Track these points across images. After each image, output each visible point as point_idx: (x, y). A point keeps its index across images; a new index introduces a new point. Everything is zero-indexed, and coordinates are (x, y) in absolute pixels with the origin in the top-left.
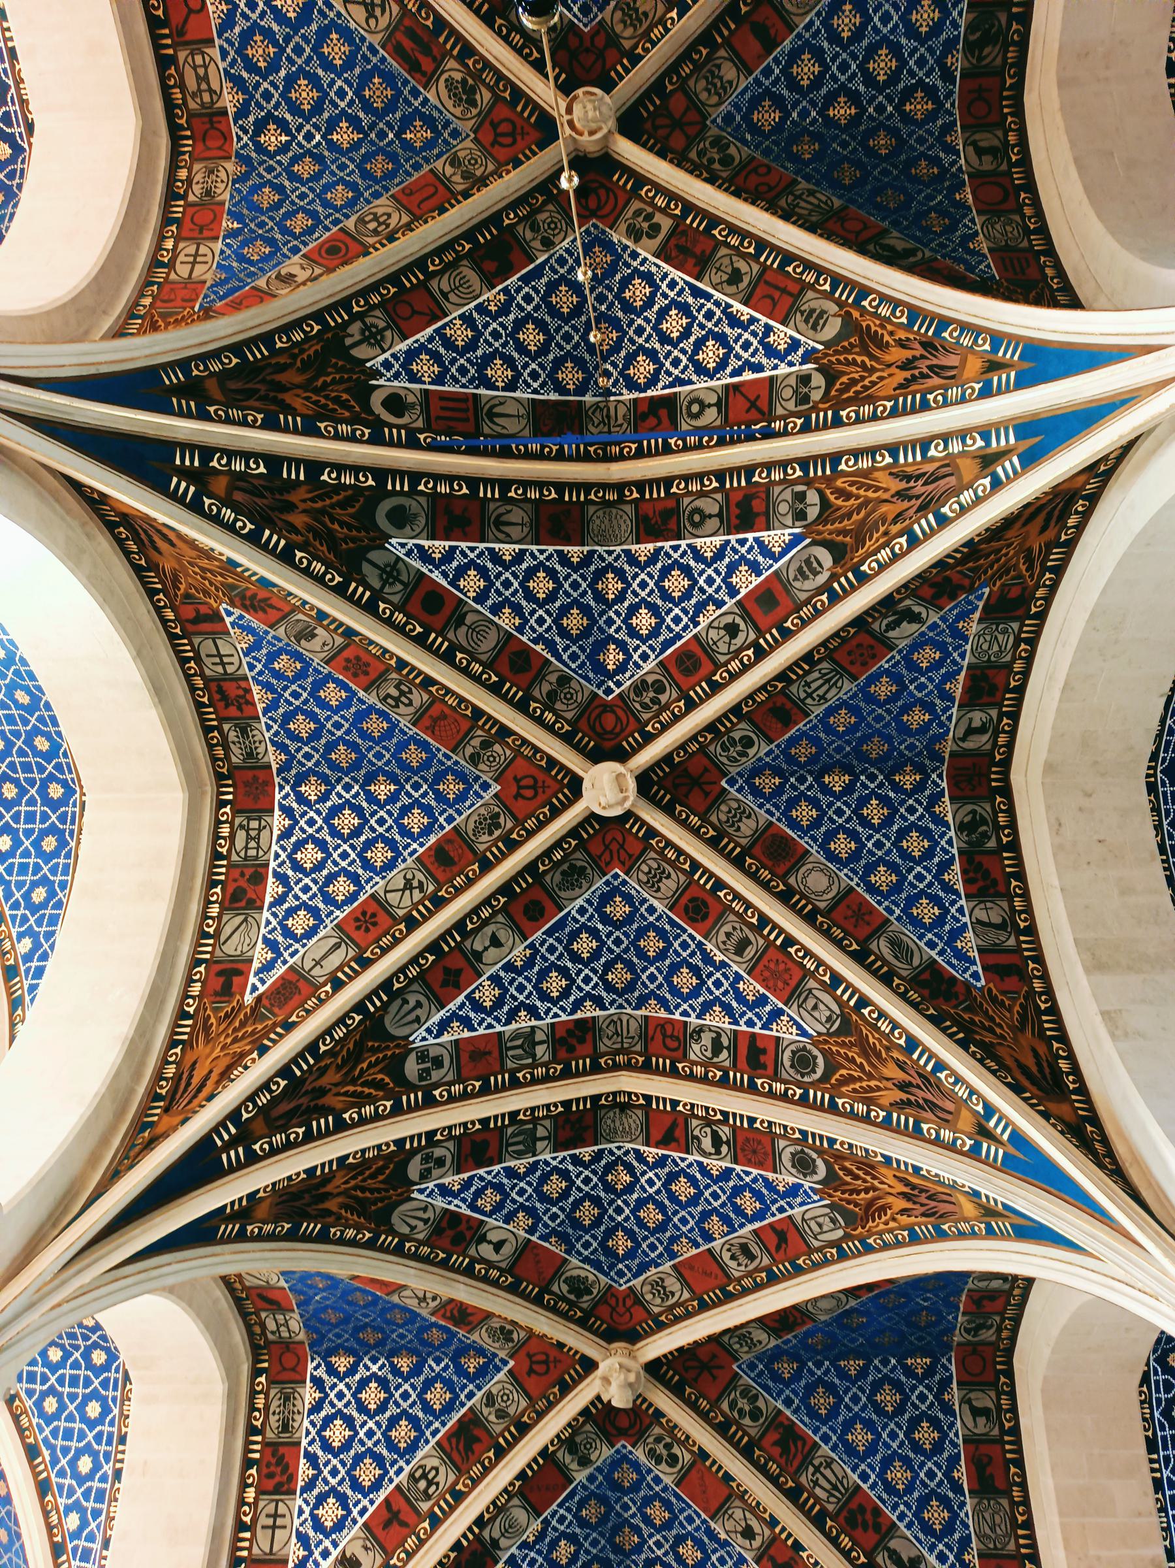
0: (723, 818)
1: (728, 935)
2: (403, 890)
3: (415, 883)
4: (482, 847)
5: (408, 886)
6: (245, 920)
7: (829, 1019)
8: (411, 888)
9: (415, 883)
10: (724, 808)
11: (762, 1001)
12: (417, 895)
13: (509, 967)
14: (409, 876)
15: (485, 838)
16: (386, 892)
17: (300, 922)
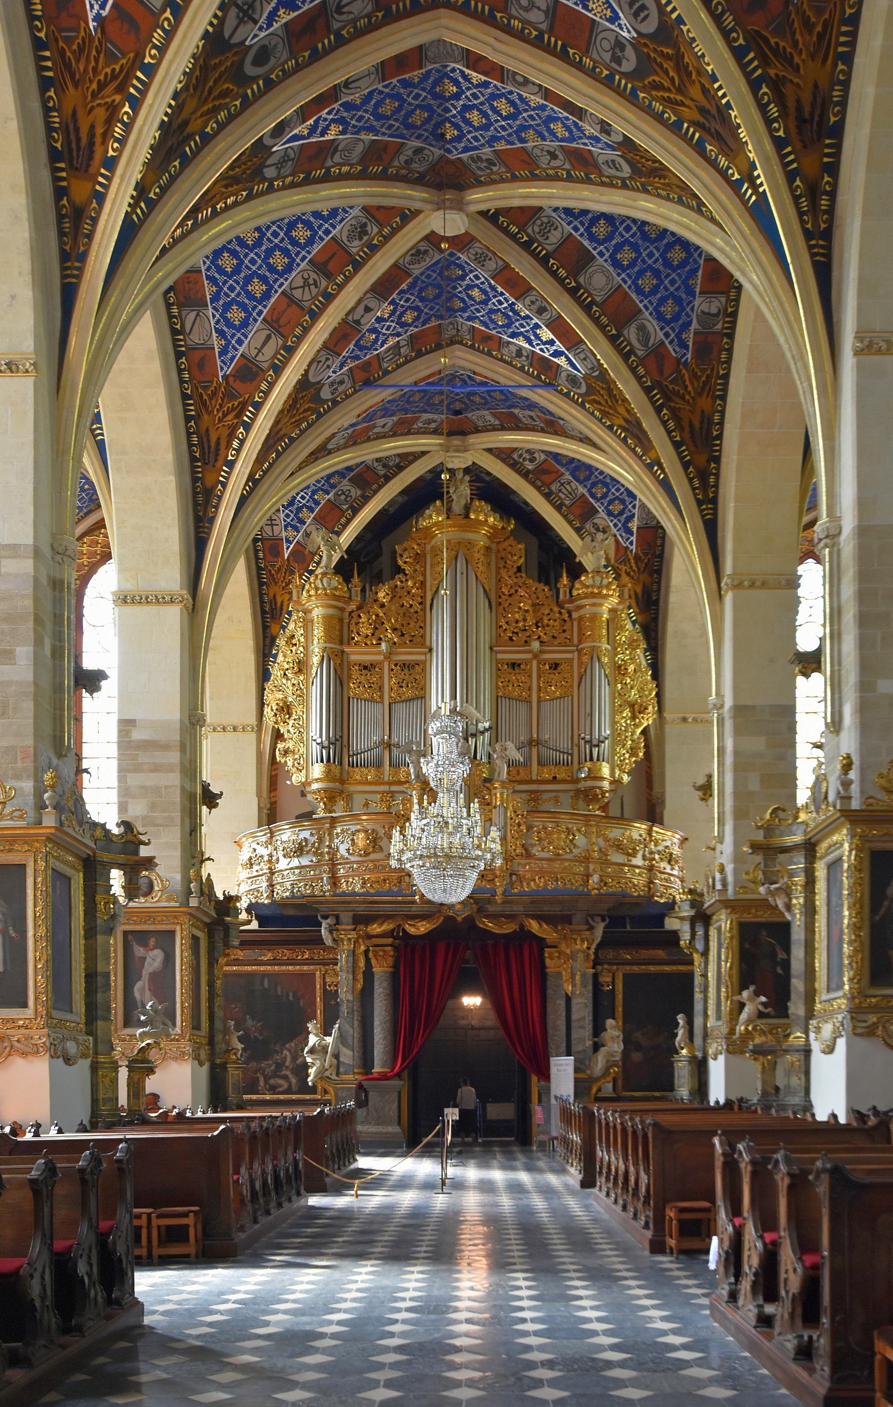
0: (537, 229)
1: (533, 302)
2: (303, 287)
3: (311, 282)
4: (354, 250)
5: (306, 284)
6: (198, 315)
7: (592, 368)
8: (309, 285)
9: (311, 282)
10: (539, 222)
11: (551, 342)
12: (314, 291)
13: (379, 320)
14: (306, 276)
15: (357, 243)
16: (291, 289)
17: (236, 315)
